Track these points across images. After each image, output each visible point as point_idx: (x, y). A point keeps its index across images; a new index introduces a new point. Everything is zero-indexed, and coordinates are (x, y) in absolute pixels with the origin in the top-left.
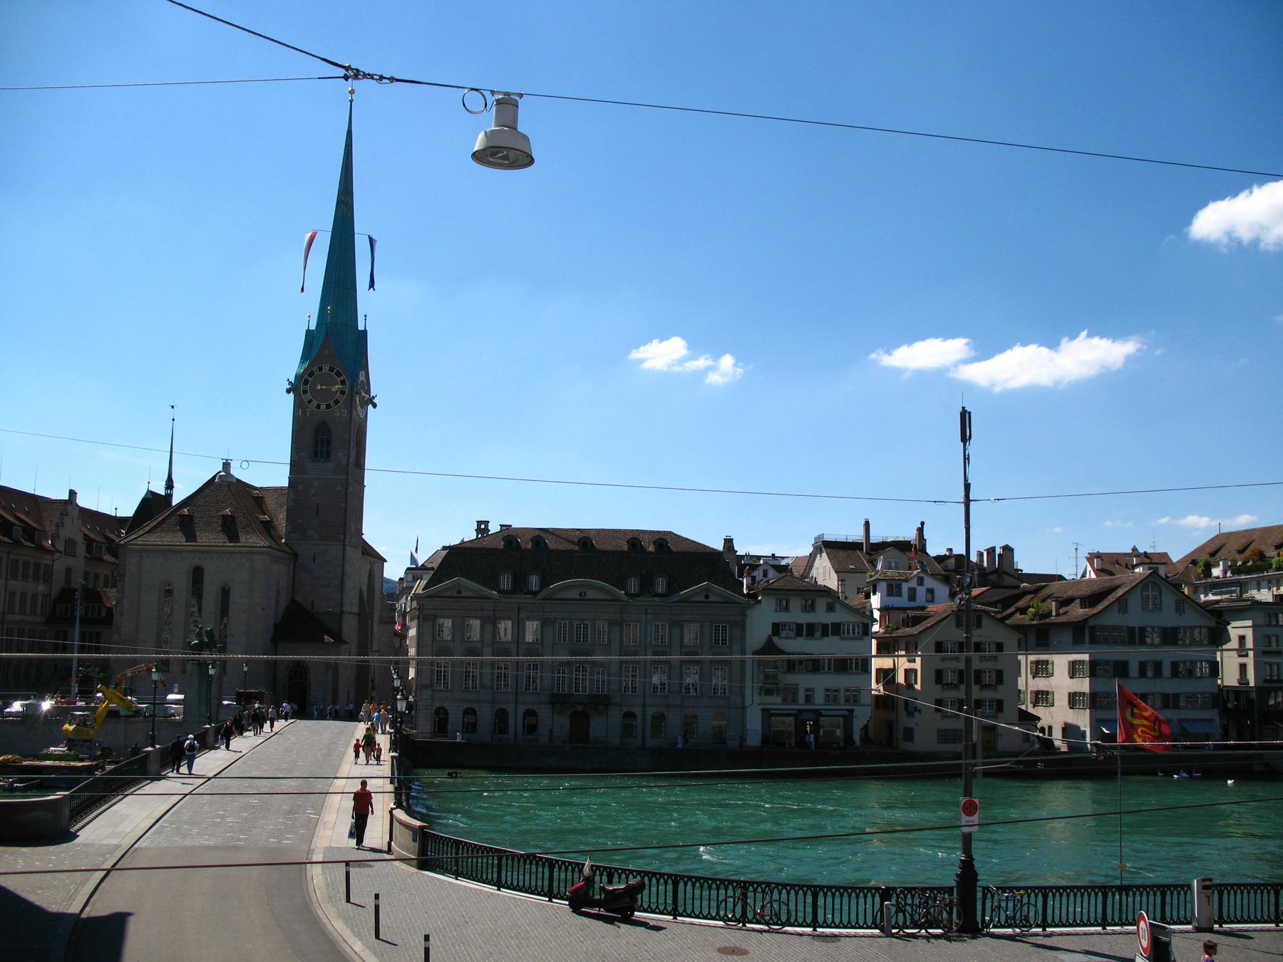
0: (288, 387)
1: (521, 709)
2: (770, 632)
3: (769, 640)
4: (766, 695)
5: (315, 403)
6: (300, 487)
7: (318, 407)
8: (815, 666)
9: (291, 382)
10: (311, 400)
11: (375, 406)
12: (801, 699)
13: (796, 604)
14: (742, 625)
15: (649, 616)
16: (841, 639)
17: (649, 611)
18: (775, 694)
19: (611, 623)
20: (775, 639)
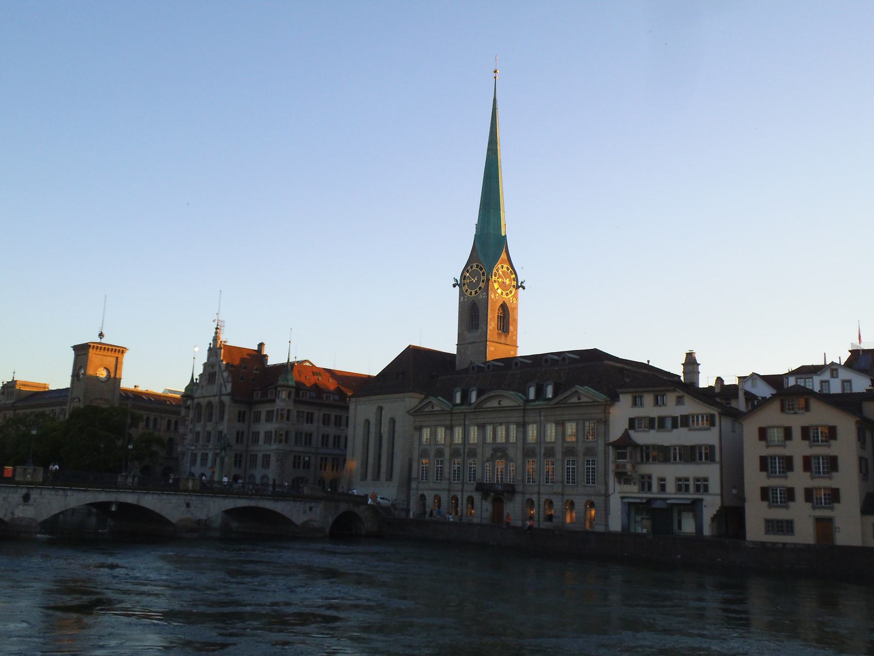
0: (454, 283)
1: (465, 497)
2: (628, 428)
3: (626, 435)
4: (624, 484)
5: (473, 292)
6: (462, 351)
7: (471, 294)
8: (664, 454)
9: (456, 280)
10: (467, 290)
11: (524, 288)
12: (655, 487)
13: (648, 399)
14: (605, 422)
15: (542, 418)
16: (689, 430)
17: (542, 414)
18: (632, 484)
19: (518, 425)
20: (631, 432)
